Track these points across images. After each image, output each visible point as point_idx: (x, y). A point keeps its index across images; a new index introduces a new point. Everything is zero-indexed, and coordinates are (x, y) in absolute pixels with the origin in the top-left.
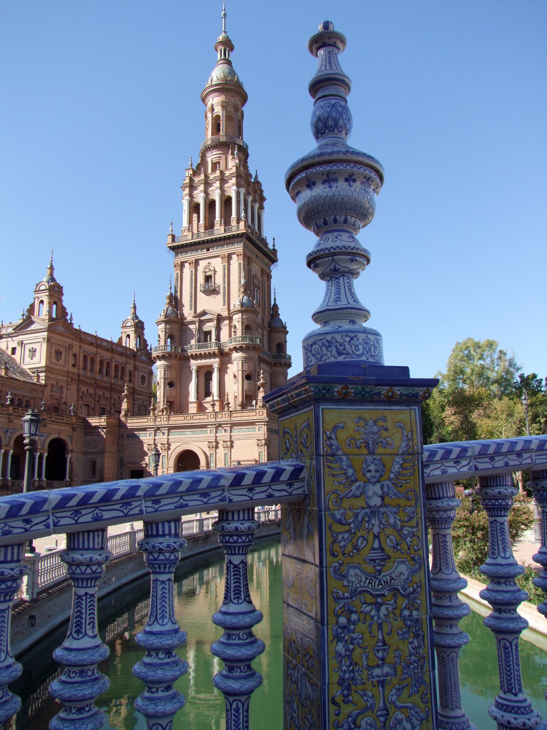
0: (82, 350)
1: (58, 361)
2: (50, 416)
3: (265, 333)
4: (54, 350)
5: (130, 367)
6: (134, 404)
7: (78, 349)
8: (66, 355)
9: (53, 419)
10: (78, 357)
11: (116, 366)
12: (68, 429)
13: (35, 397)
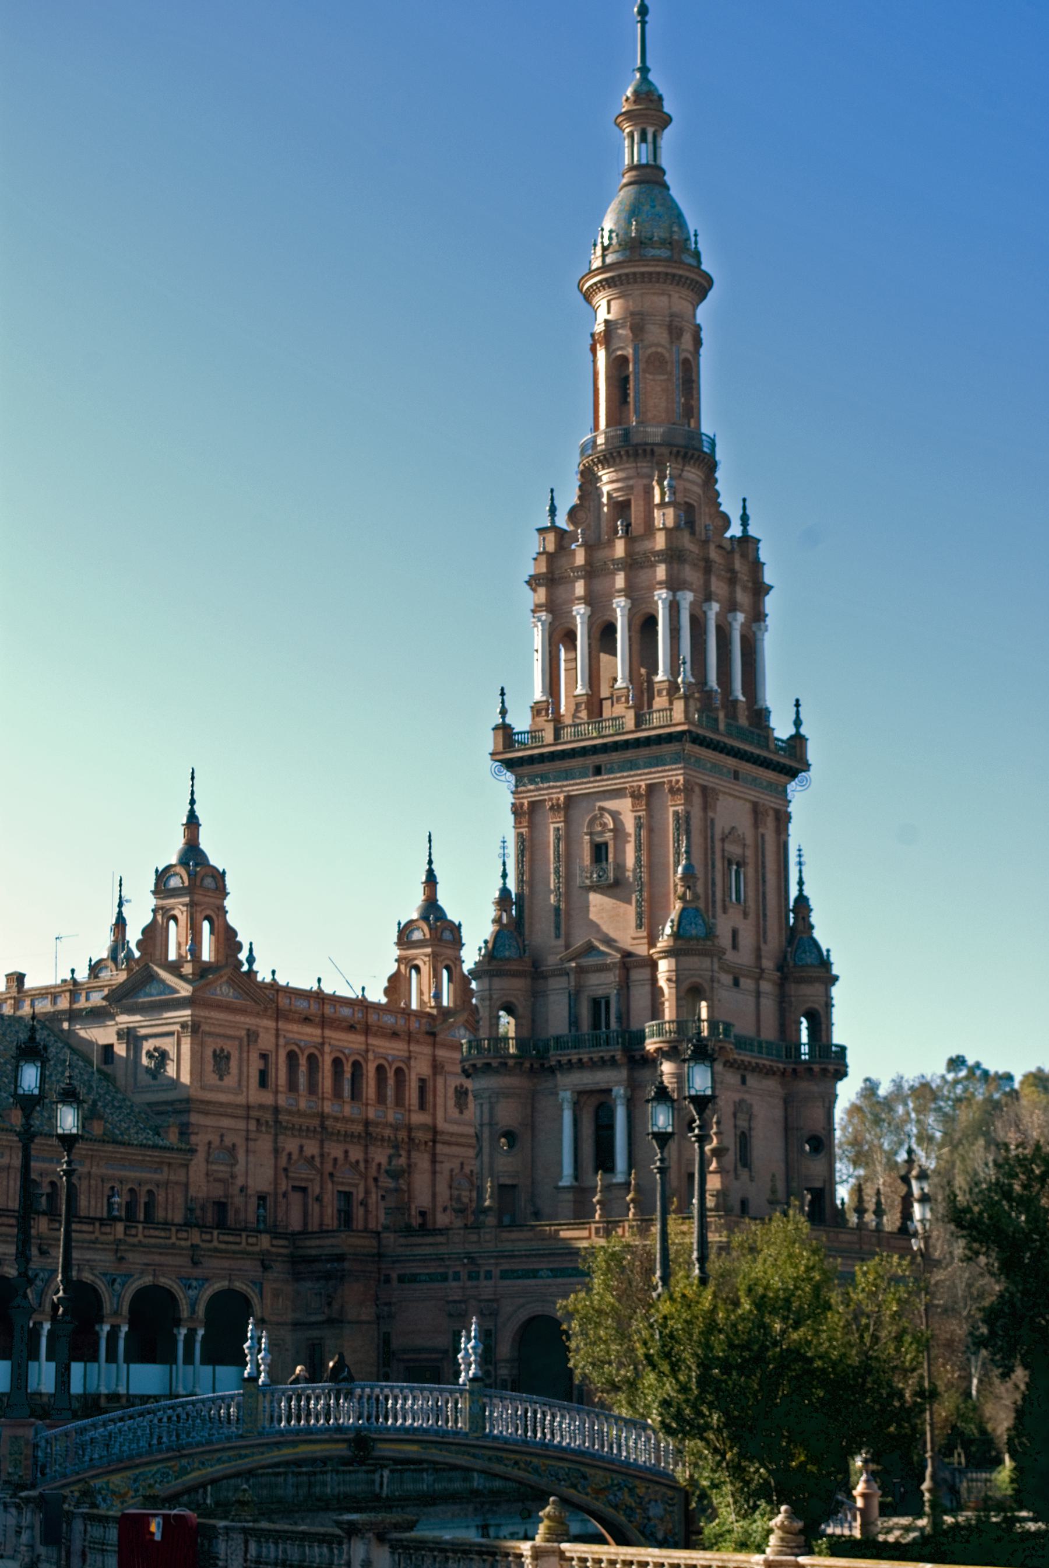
0: (282, 1041)
1: (221, 1079)
2: (207, 1237)
3: (766, 986)
4: (209, 1052)
5: (421, 1068)
6: (434, 1173)
7: (273, 1039)
8: (240, 1059)
9: (215, 1244)
10: (272, 1059)
11: (380, 1069)
12: (251, 1267)
13: (167, 1182)
